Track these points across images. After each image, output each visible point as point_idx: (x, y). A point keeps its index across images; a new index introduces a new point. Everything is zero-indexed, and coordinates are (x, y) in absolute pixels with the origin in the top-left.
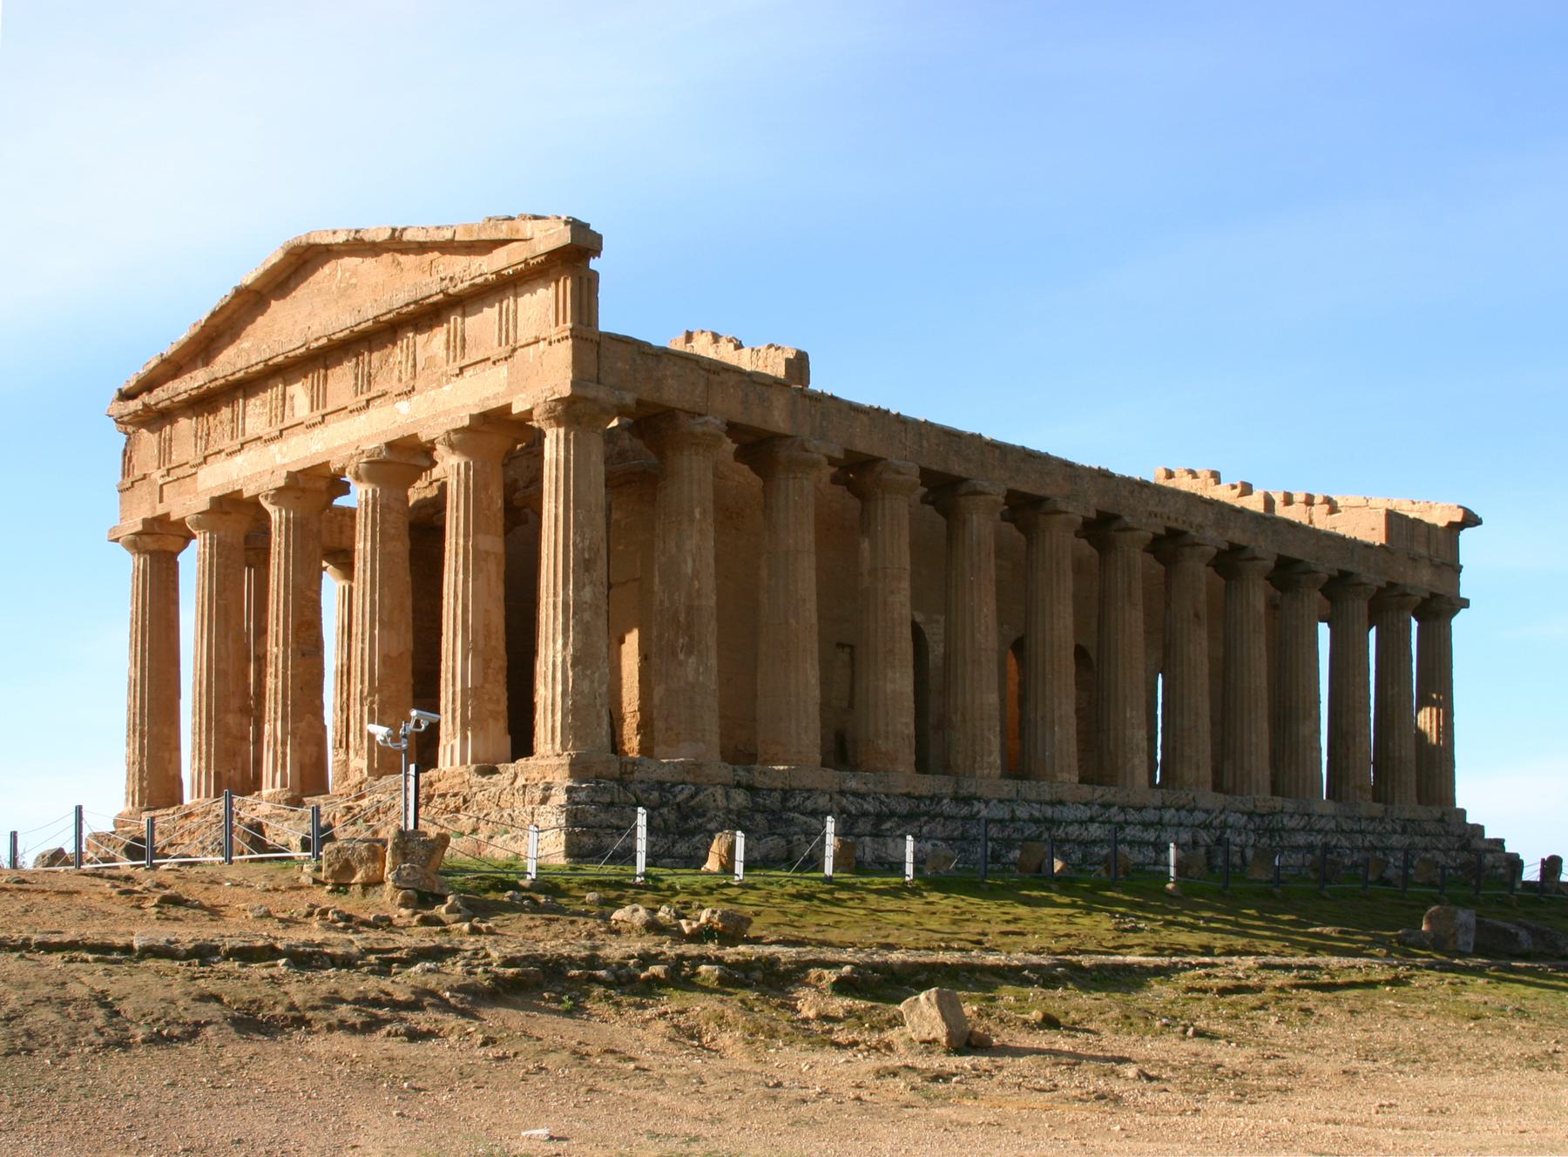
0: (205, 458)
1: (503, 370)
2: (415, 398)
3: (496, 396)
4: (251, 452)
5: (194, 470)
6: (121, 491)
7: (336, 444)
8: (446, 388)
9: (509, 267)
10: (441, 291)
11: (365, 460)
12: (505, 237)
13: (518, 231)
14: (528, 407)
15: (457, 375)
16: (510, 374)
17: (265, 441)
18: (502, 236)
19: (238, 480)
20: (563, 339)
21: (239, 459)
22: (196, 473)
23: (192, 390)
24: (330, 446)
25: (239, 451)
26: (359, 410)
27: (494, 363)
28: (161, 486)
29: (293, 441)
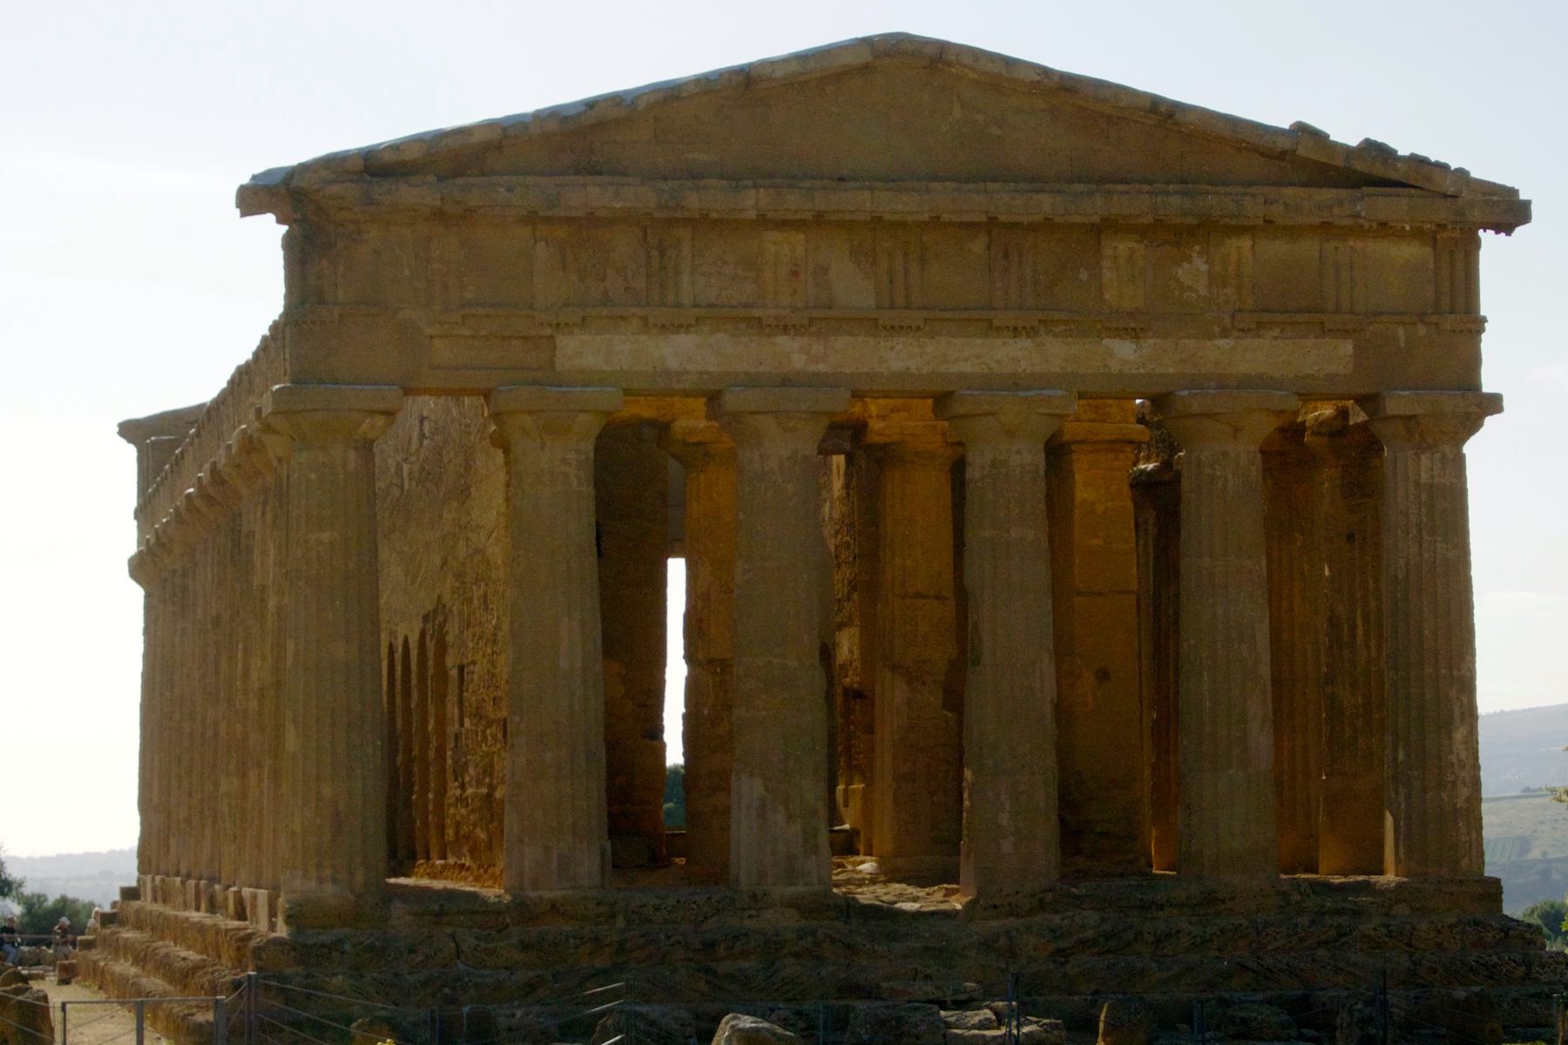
0: (584, 319)
1: (1347, 348)
2: (1149, 343)
3: (1332, 377)
4: (718, 336)
5: (549, 331)
7: (954, 369)
12: (1404, 181)
18: (1394, 176)
19: (679, 374)
22: (552, 337)
24: (942, 369)
25: (690, 326)
26: (1016, 332)
28: (431, 337)
29: (842, 342)
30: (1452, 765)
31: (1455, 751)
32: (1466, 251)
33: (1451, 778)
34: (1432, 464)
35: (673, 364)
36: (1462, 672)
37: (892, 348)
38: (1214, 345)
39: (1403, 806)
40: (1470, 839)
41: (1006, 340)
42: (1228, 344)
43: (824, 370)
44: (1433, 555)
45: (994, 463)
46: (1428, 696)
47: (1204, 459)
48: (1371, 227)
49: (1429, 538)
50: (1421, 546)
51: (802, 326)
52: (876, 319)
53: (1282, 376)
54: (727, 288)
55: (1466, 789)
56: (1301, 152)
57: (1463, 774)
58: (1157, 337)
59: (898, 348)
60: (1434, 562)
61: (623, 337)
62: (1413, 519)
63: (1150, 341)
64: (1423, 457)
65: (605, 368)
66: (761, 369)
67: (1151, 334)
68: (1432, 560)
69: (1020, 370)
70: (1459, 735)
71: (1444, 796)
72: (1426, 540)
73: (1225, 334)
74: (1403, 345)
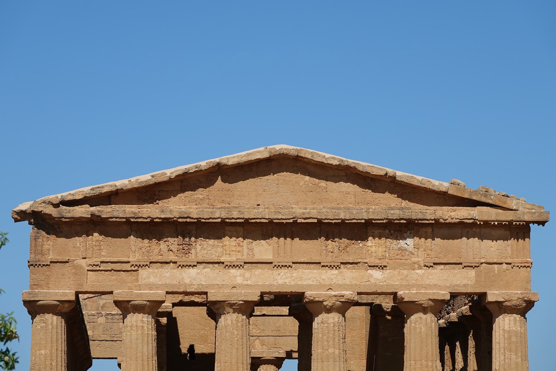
1: (472, 273)
2: (387, 272)
5: (136, 268)
6: (31, 265)
7: (305, 283)
8: (416, 271)
9: (496, 221)
10: (434, 219)
11: (343, 300)
13: (505, 203)
14: (502, 300)
15: (431, 266)
16: (478, 275)
17: (227, 265)
18: (491, 202)
20: (525, 266)
21: (192, 271)
23: (157, 218)
24: (300, 283)
25: (194, 266)
27: (465, 266)
28: (88, 270)
32: (524, 233)
35: (187, 281)
37: (279, 274)
41: (327, 271)
43: (250, 284)
45: (322, 322)
48: (480, 223)
51: (241, 265)
52: (272, 263)
54: (210, 250)
56: (450, 192)
59: (281, 274)
61: (167, 270)
65: (159, 283)
66: (224, 283)
67: (388, 268)
69: (333, 283)
73: (420, 268)
74: (496, 272)
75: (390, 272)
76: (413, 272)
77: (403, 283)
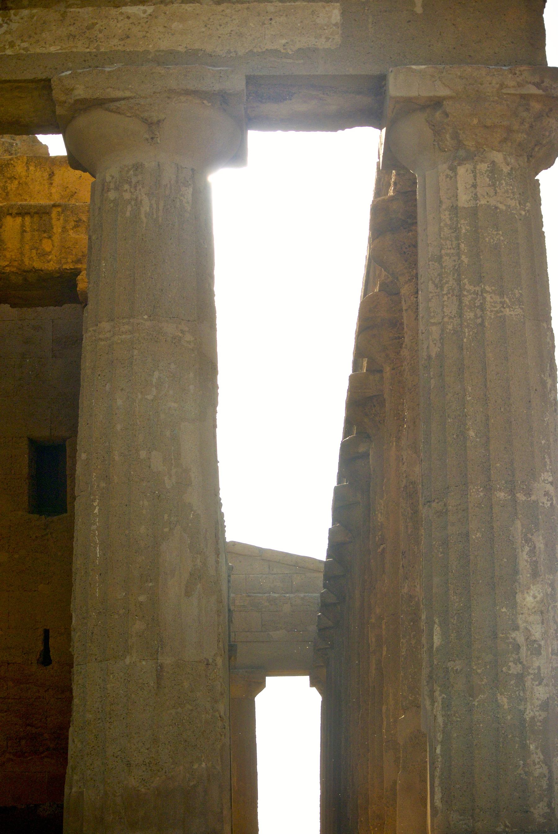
30: (517, 647)
31: (522, 625)
33: (515, 669)
34: (475, 178)
36: (533, 498)
38: (121, 13)
39: (440, 720)
40: (550, 772)
42: (145, 12)
44: (479, 313)
46: (476, 536)
47: (108, 179)
49: (471, 288)
50: (461, 302)
53: (229, 52)
55: (541, 689)
57: (536, 664)
58: (35, 6)
60: (482, 324)
62: (448, 262)
63: (25, 12)
64: (461, 170)
68: (479, 321)
70: (529, 599)
71: (503, 700)
72: (468, 291)
75: (32, 17)
76: (114, 12)
77: (74, 50)
